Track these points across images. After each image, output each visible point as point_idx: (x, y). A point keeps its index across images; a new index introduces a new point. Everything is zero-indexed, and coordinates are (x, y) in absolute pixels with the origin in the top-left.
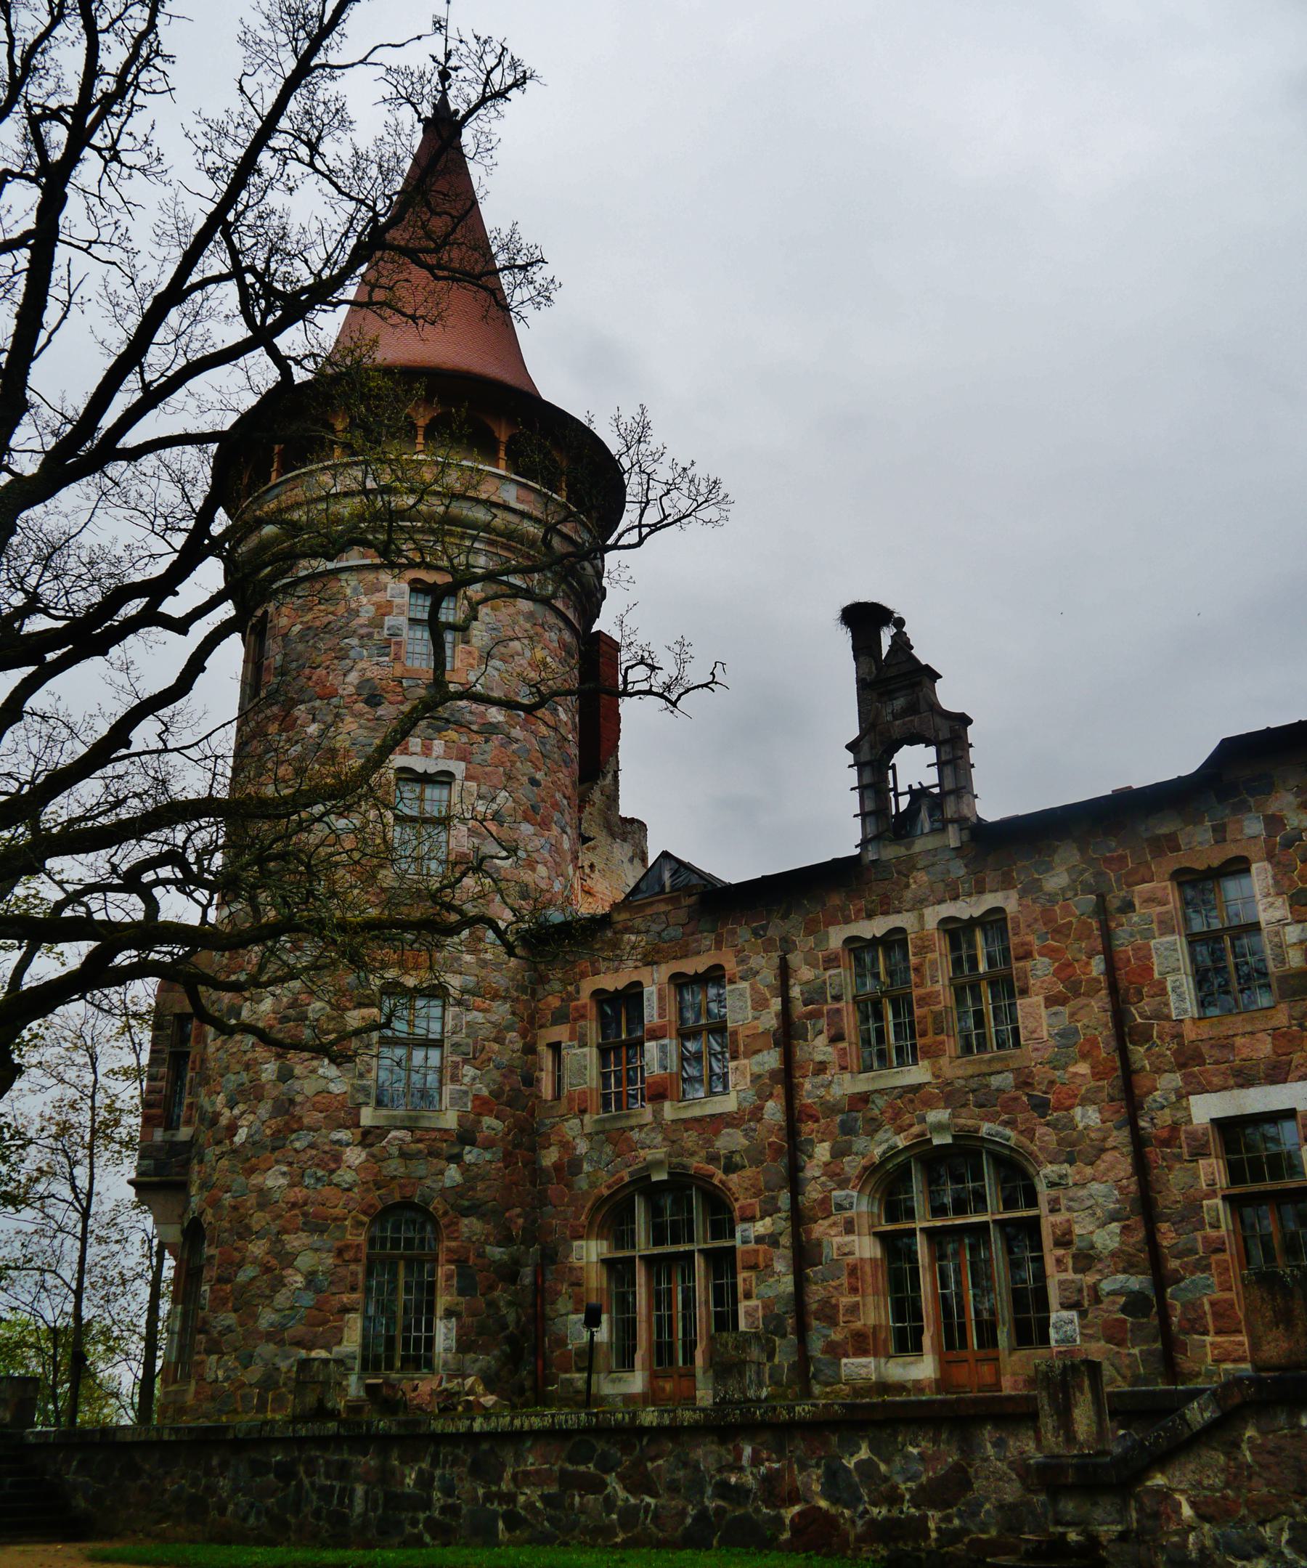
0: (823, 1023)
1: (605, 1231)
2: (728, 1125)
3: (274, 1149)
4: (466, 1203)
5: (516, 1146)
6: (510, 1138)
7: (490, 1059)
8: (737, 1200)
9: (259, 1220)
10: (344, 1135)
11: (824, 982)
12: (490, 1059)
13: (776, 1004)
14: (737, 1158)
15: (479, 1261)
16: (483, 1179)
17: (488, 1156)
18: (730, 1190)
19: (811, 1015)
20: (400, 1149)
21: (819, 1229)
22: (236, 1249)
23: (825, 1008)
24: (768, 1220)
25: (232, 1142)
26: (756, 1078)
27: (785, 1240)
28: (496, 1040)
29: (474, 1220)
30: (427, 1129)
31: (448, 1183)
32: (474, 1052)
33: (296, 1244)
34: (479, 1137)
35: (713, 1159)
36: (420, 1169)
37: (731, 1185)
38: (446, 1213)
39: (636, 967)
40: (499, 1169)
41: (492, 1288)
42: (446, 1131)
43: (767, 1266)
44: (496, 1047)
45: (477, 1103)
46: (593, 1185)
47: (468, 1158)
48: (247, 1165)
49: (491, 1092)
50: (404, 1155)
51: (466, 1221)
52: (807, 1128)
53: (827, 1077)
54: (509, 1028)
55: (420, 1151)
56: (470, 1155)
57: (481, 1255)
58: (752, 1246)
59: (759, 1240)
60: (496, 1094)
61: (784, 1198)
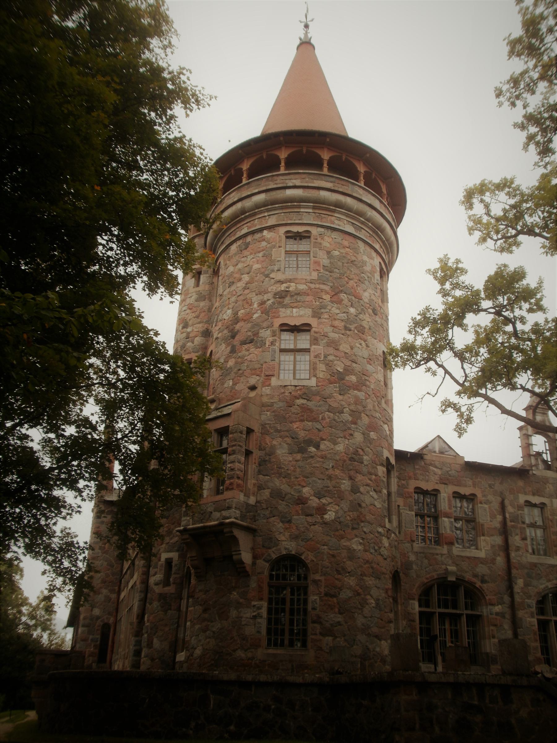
0: (518, 531)
2: (482, 563)
3: (353, 529)
8: (487, 595)
9: (350, 566)
11: (518, 515)
13: (499, 518)
14: (486, 578)
18: (484, 591)
19: (513, 527)
21: (520, 614)
22: (336, 579)
23: (519, 525)
24: (500, 606)
25: (322, 518)
26: (493, 546)
27: (508, 616)
33: (370, 582)
35: (475, 576)
37: (484, 588)
39: (437, 483)
43: (501, 626)
48: (337, 533)
52: (514, 571)
53: (520, 553)
58: (494, 616)
59: (497, 614)
61: (507, 599)
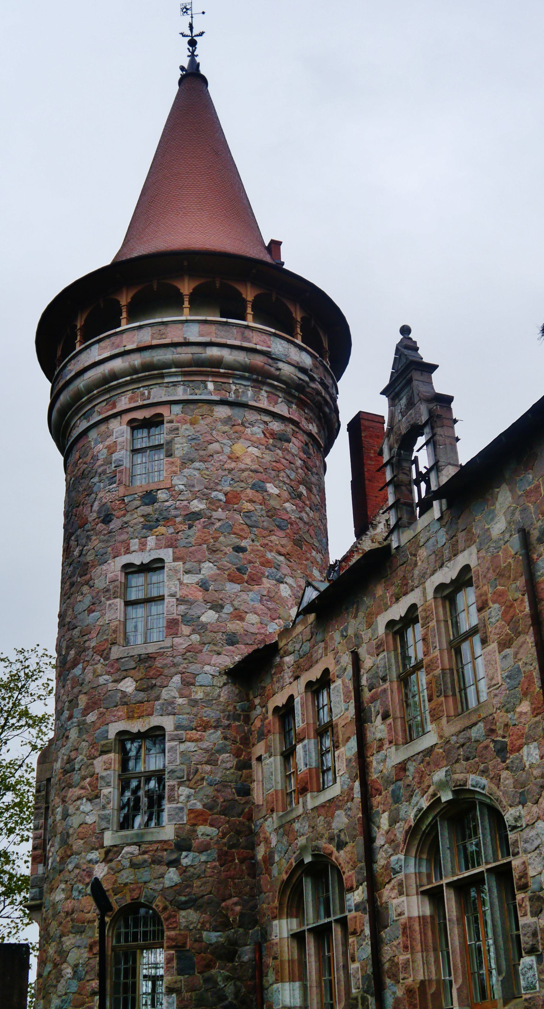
1: (294, 910)
4: (183, 899)
5: (231, 847)
6: (225, 840)
7: (203, 779)
10: (94, 855)
12: (203, 779)
15: (196, 945)
16: (199, 877)
17: (203, 858)
20: (131, 861)
28: (208, 763)
29: (191, 911)
30: (151, 843)
31: (167, 884)
32: (188, 775)
34: (195, 843)
36: (145, 875)
38: (165, 908)
40: (215, 867)
41: (209, 966)
42: (165, 842)
44: (208, 768)
45: (192, 815)
46: (280, 873)
47: (185, 862)
49: (204, 806)
50: (134, 865)
51: (183, 913)
54: (221, 751)
55: (145, 861)
56: (186, 859)
57: (199, 940)
60: (209, 807)
